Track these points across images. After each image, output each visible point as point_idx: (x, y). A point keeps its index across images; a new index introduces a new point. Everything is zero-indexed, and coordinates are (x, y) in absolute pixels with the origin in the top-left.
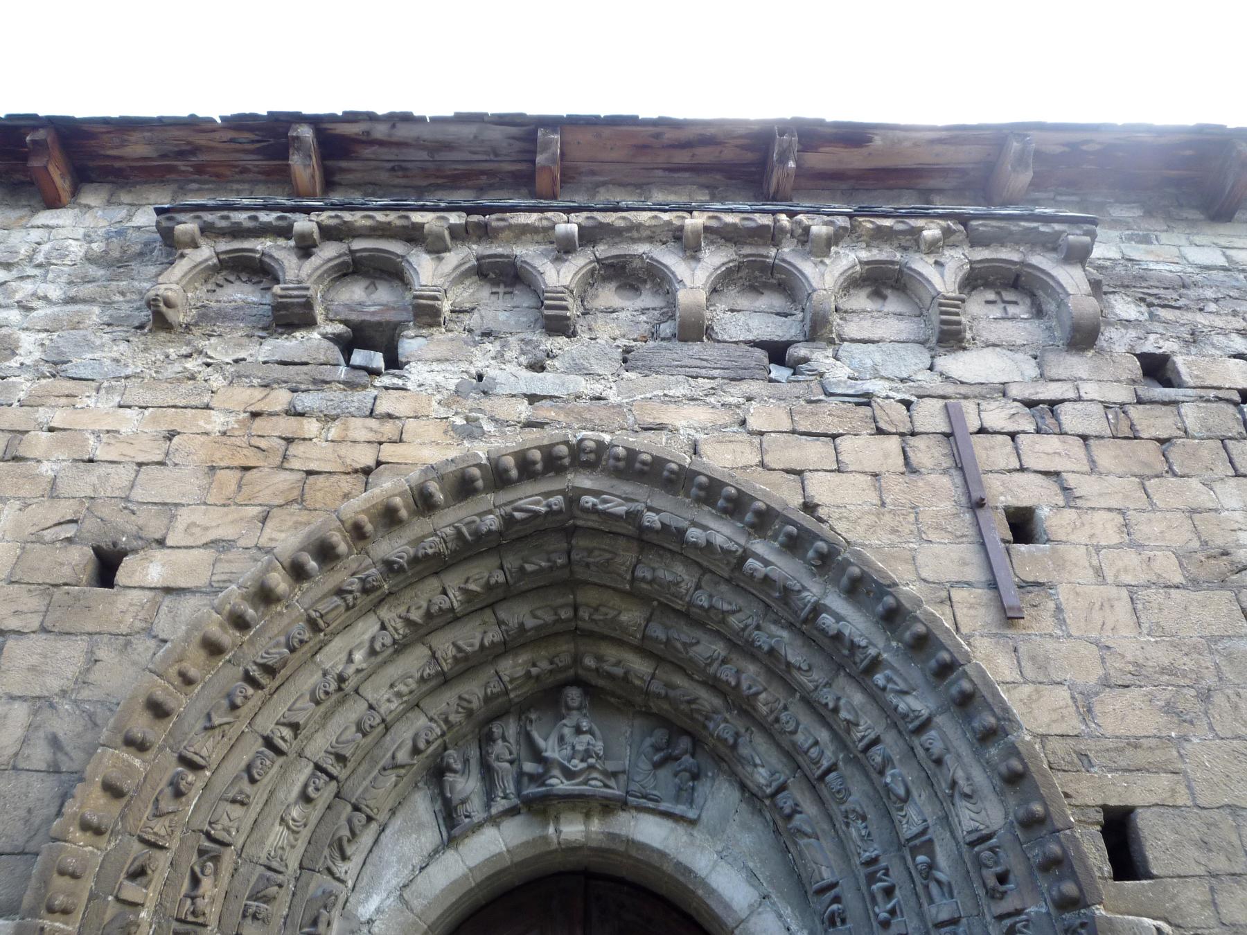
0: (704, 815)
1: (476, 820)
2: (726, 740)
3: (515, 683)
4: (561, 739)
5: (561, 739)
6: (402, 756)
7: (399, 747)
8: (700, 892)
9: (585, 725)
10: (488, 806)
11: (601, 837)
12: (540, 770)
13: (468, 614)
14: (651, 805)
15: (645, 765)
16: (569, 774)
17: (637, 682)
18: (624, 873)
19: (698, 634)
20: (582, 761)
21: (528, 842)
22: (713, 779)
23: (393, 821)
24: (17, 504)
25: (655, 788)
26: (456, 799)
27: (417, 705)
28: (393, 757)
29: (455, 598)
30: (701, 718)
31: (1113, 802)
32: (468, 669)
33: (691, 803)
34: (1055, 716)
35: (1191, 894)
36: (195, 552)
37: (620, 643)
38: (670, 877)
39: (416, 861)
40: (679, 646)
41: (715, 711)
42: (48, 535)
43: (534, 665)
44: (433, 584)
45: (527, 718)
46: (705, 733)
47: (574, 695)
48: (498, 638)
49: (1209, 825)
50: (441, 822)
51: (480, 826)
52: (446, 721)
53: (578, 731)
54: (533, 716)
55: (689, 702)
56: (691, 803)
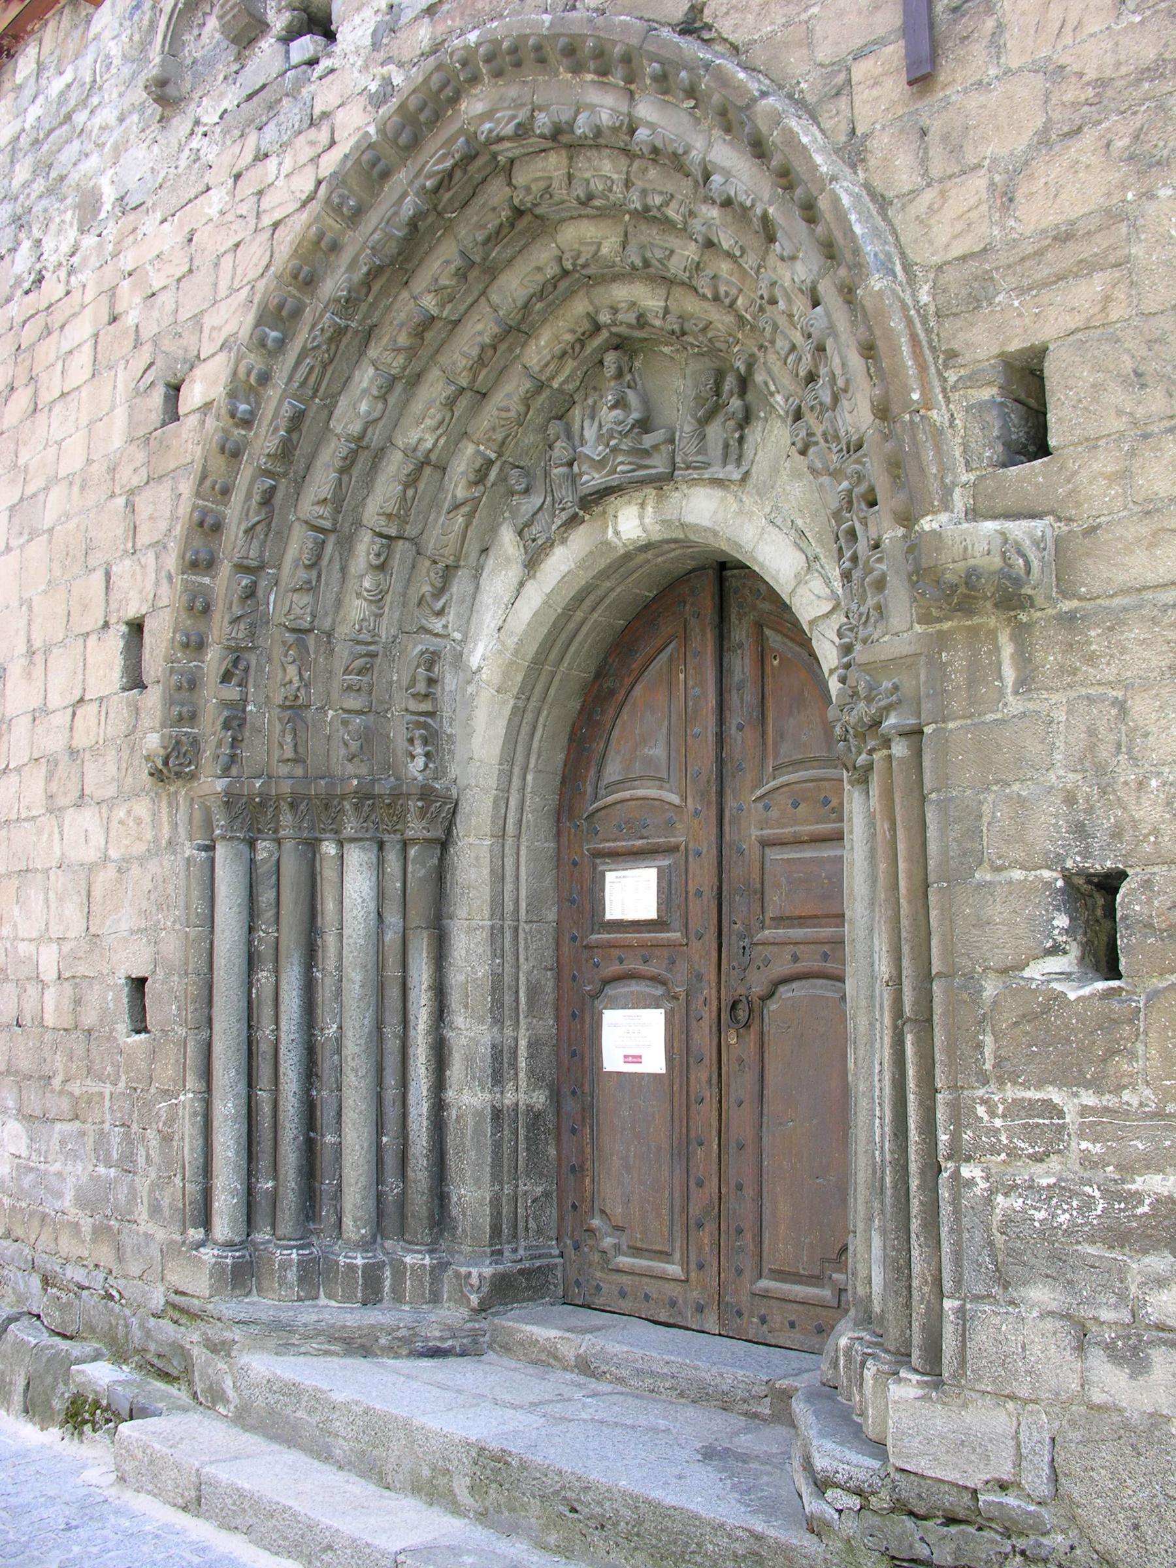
11: (658, 527)
21: (591, 552)
22: (766, 419)
24: (122, 363)
28: (454, 496)
29: (429, 302)
31: (1014, 346)
34: (960, 226)
35: (1096, 466)
36: (217, 357)
42: (142, 385)
44: (405, 295)
49: (1150, 343)
55: (704, 330)
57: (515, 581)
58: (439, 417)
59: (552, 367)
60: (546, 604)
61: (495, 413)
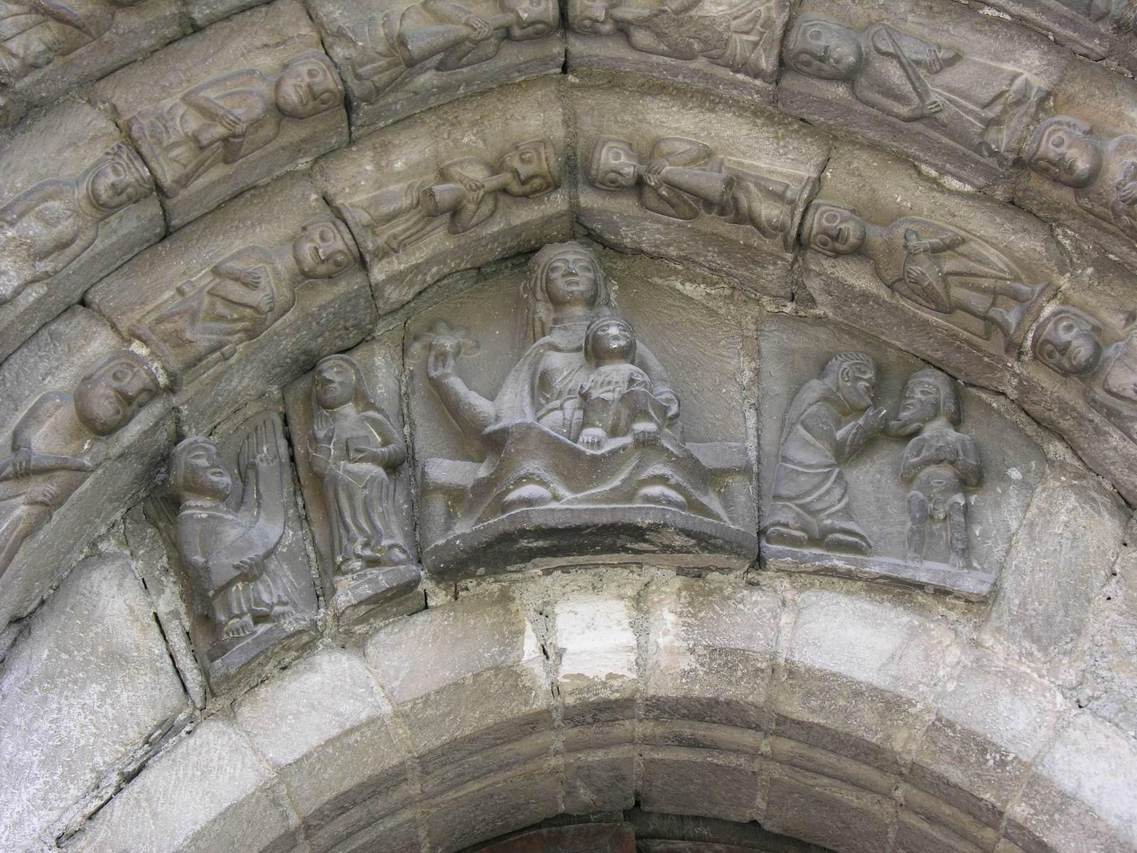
0: (1008, 584)
1: (289, 626)
2: (1064, 349)
3: (386, 233)
4: (542, 385)
5: (542, 385)
6: (44, 441)
7: (33, 415)
8: (1019, 810)
9: (614, 333)
10: (321, 594)
12: (483, 471)
13: (227, 17)
14: (839, 561)
15: (808, 454)
16: (576, 466)
17: (768, 211)
18: (758, 807)
19: (959, 35)
20: (614, 432)
21: (457, 685)
22: (1027, 486)
23: (25, 651)
25: (847, 513)
26: (222, 565)
27: (83, 303)
28: (17, 443)
30: (978, 302)
32: (240, 194)
33: (966, 551)
37: (705, 97)
38: (914, 774)
39: (108, 755)
40: (893, 73)
41: (1025, 267)
43: (443, 176)
45: (430, 347)
46: (995, 345)
47: (569, 263)
48: (328, 81)
50: (178, 642)
51: (304, 645)
52: (179, 341)
53: (595, 353)
54: (448, 342)
56: (966, 551)
57: (148, 719)
58: (65, 227)
59: (399, 227)
60: (269, 794)
61: (203, 278)
